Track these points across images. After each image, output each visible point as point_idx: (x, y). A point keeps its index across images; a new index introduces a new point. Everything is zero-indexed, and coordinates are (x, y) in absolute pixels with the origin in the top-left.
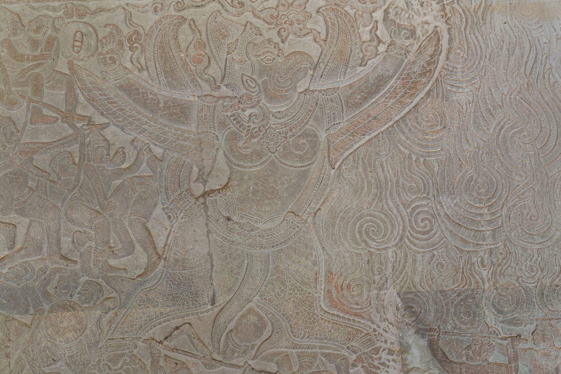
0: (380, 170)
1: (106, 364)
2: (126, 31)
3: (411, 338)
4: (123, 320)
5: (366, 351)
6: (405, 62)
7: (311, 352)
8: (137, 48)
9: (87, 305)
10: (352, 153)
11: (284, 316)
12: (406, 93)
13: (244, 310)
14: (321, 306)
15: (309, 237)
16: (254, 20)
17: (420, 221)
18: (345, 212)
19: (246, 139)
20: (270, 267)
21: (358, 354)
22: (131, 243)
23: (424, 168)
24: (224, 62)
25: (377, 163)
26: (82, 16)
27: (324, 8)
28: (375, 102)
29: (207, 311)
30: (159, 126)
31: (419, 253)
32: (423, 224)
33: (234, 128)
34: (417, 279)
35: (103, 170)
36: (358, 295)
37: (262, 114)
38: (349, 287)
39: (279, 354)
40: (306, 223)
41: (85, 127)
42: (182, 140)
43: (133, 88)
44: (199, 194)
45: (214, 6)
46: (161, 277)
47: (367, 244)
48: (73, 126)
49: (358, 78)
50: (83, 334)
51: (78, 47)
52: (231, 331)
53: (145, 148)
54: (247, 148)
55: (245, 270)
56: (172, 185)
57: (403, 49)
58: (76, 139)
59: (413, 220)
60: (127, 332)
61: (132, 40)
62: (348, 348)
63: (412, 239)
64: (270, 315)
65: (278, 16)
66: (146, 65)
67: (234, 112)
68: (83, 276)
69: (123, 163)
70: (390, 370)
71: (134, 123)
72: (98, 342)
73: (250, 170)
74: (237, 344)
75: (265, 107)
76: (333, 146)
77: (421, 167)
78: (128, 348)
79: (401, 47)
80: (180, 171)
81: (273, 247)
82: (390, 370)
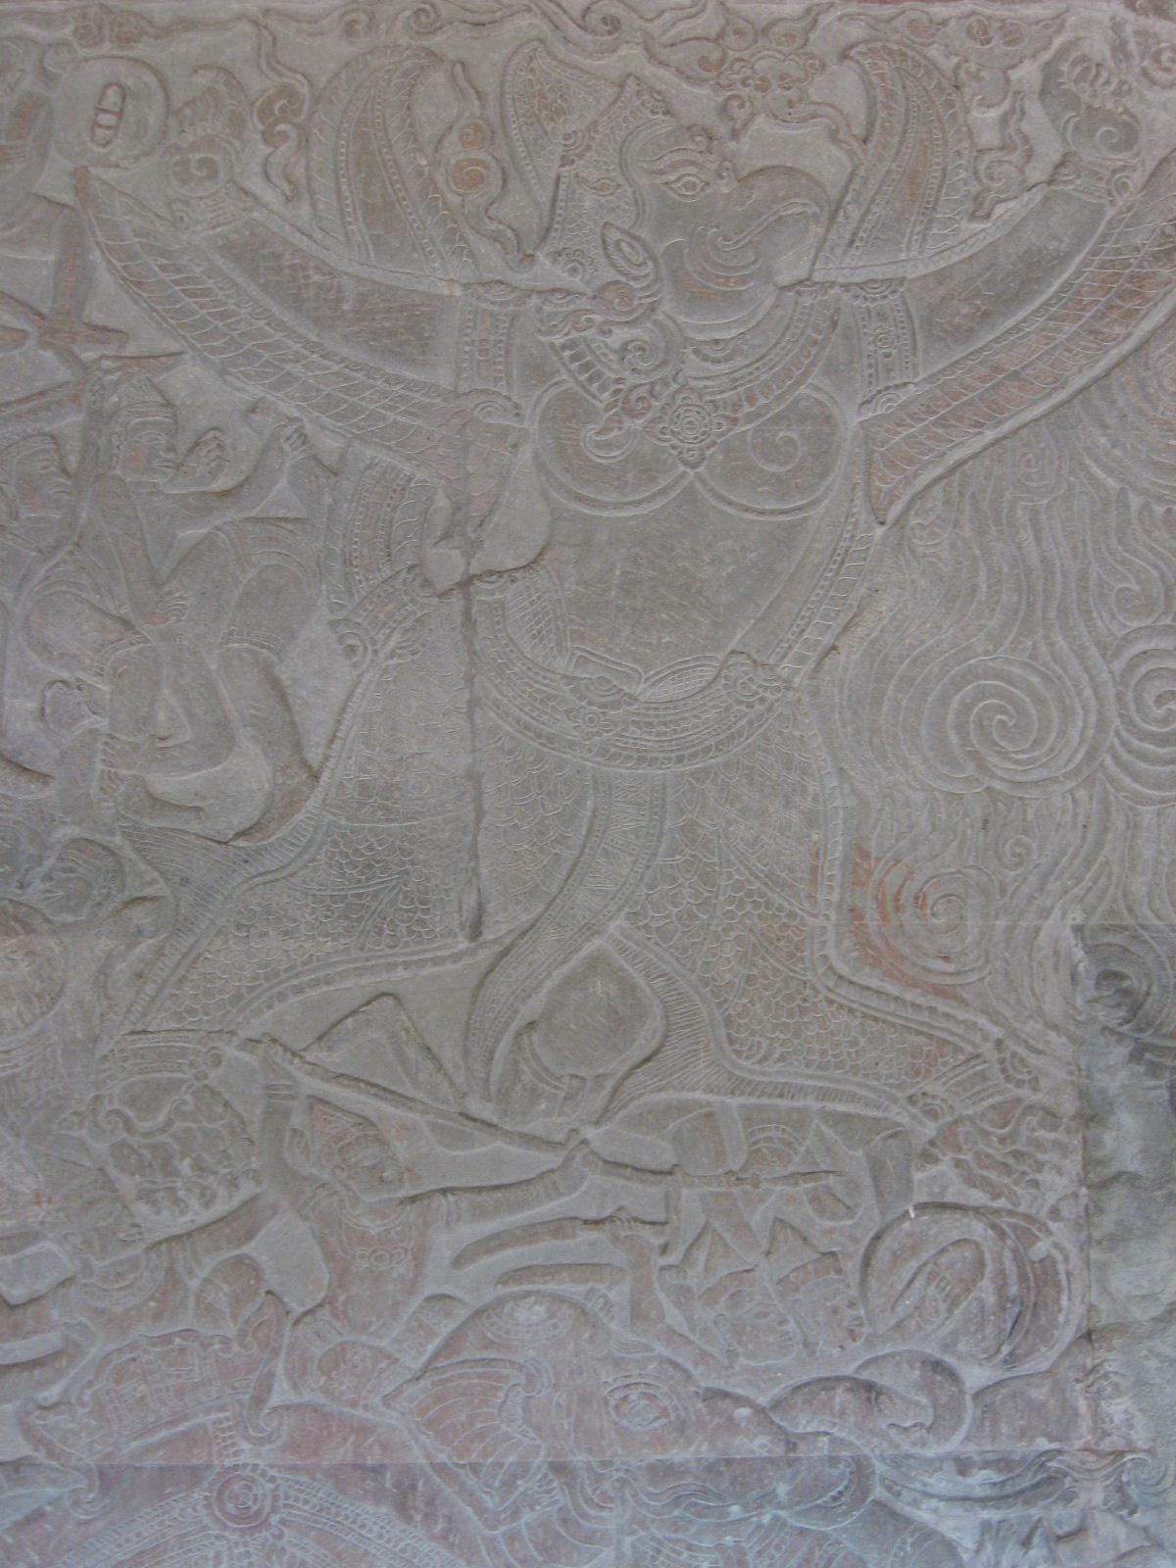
0: (1026, 535)
1: (117, 1113)
2: (258, 84)
3: (1115, 1072)
4: (181, 971)
5: (970, 1112)
6: (1107, 218)
7: (790, 1110)
8: (285, 136)
9: (69, 918)
10: (941, 478)
11: (707, 985)
12: (1110, 307)
13: (575, 961)
14: (825, 957)
15: (797, 733)
16: (649, 70)
17: (1151, 703)
18: (914, 661)
19: (609, 419)
20: (668, 824)
21: (941, 1122)
22: (223, 725)
23: (1166, 536)
24: (550, 187)
25: (1020, 512)
26: (128, 40)
27: (862, 48)
28: (1016, 328)
29: (456, 958)
30: (336, 368)
31: (1148, 801)
32: (1160, 712)
33: (570, 384)
34: (1139, 885)
35: (151, 494)
36: (950, 929)
37: (662, 344)
38: (919, 900)
39: (684, 1108)
40: (788, 689)
41: (107, 364)
42: (406, 413)
43: (266, 252)
44: (447, 585)
45: (527, 24)
46: (311, 841)
47: (983, 767)
48: (72, 359)
49: (965, 255)
50: (50, 1009)
51: (108, 127)
52: (531, 1025)
53: (288, 431)
54: (609, 446)
55: (584, 831)
56: (365, 551)
57: (1101, 179)
58: (75, 398)
59: (1130, 697)
60: (190, 1011)
61: (273, 114)
62: (911, 1100)
63: (1126, 757)
64: (660, 982)
65: (723, 61)
66: (309, 185)
67: (574, 335)
68: (65, 823)
69: (214, 477)
70: (1046, 1177)
71: (260, 356)
72: (96, 1040)
73: (617, 514)
74: (546, 1069)
75: (671, 325)
76: (882, 454)
77: (1156, 534)
78: (192, 1064)
79: (1097, 173)
80: (394, 509)
81: (680, 760)
82: (1046, 1177)
